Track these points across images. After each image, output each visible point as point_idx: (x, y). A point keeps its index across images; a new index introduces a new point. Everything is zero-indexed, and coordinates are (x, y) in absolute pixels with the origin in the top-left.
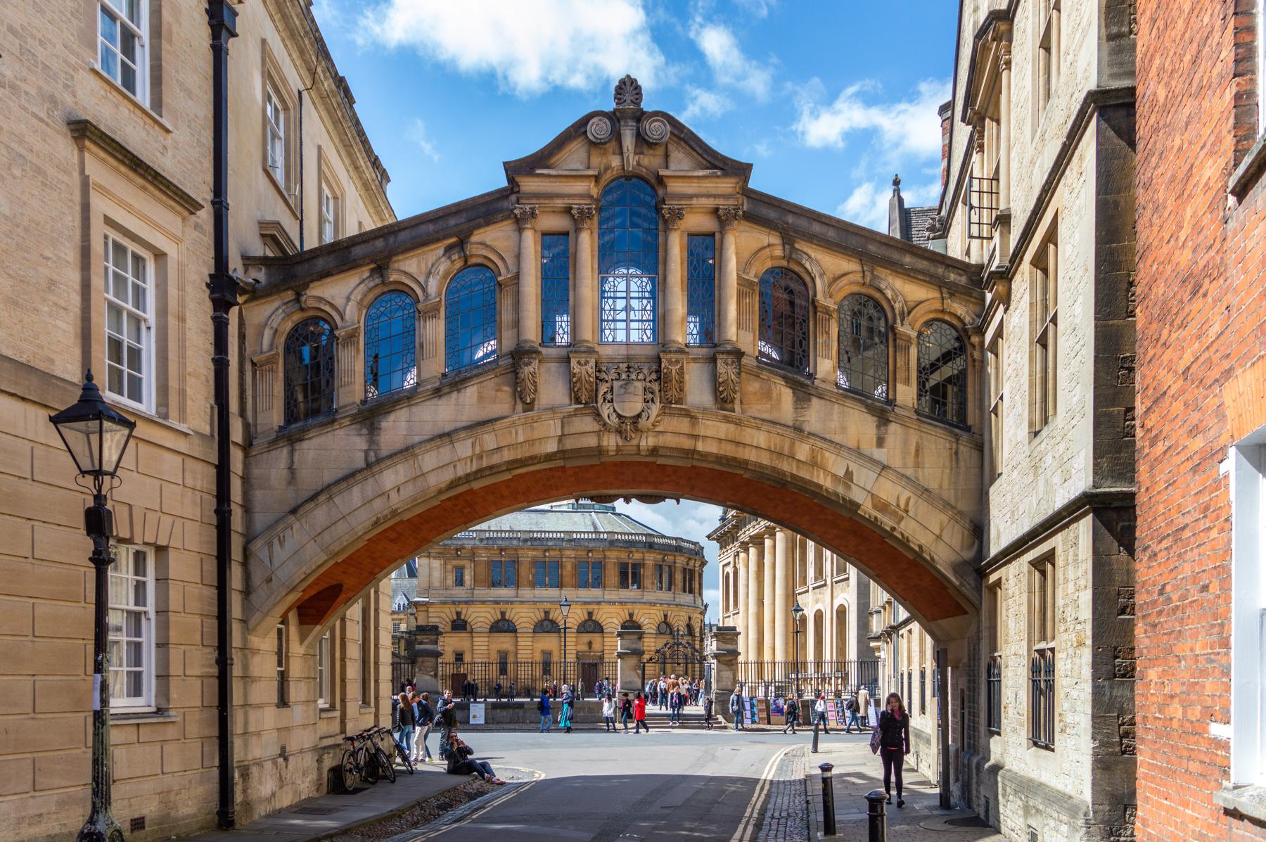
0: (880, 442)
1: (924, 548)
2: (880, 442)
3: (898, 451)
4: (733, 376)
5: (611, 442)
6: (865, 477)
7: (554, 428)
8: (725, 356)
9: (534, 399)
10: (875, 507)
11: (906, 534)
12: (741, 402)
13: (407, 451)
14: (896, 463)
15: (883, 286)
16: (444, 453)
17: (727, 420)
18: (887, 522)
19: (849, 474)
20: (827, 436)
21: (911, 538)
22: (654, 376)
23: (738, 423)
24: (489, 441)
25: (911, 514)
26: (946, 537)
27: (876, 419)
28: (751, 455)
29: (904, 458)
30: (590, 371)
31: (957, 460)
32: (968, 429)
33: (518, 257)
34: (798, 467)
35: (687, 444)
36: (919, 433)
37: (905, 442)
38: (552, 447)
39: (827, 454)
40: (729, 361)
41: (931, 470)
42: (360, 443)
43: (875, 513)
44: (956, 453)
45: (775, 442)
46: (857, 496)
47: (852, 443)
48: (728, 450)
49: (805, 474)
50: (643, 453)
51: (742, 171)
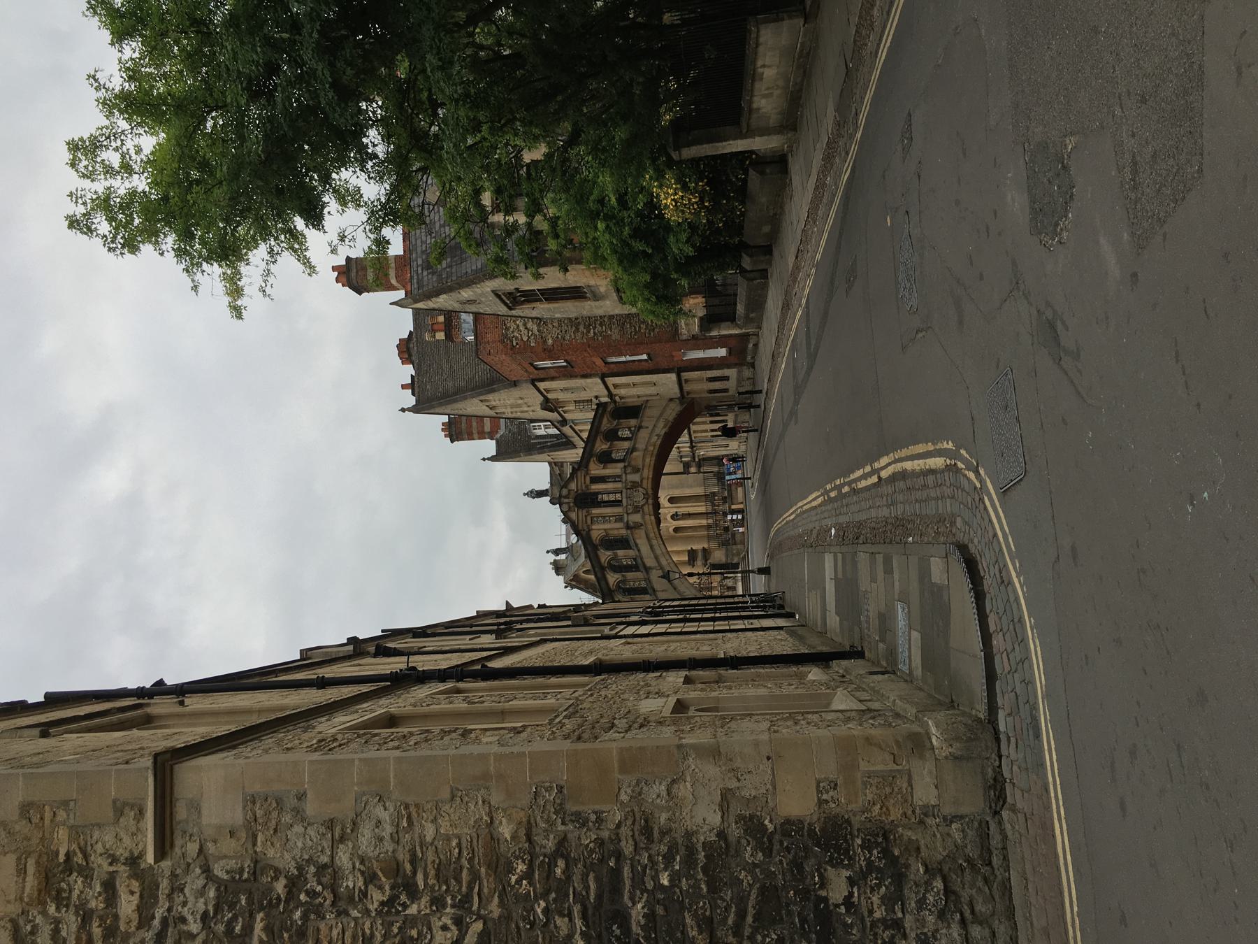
0: (647, 427)
2: (647, 427)
5: (650, 501)
6: (657, 431)
7: (647, 517)
13: (657, 558)
14: (653, 423)
16: (656, 547)
18: (670, 424)
23: (643, 466)
24: (652, 535)
28: (653, 463)
33: (599, 530)
35: (650, 480)
38: (653, 518)
42: (654, 571)
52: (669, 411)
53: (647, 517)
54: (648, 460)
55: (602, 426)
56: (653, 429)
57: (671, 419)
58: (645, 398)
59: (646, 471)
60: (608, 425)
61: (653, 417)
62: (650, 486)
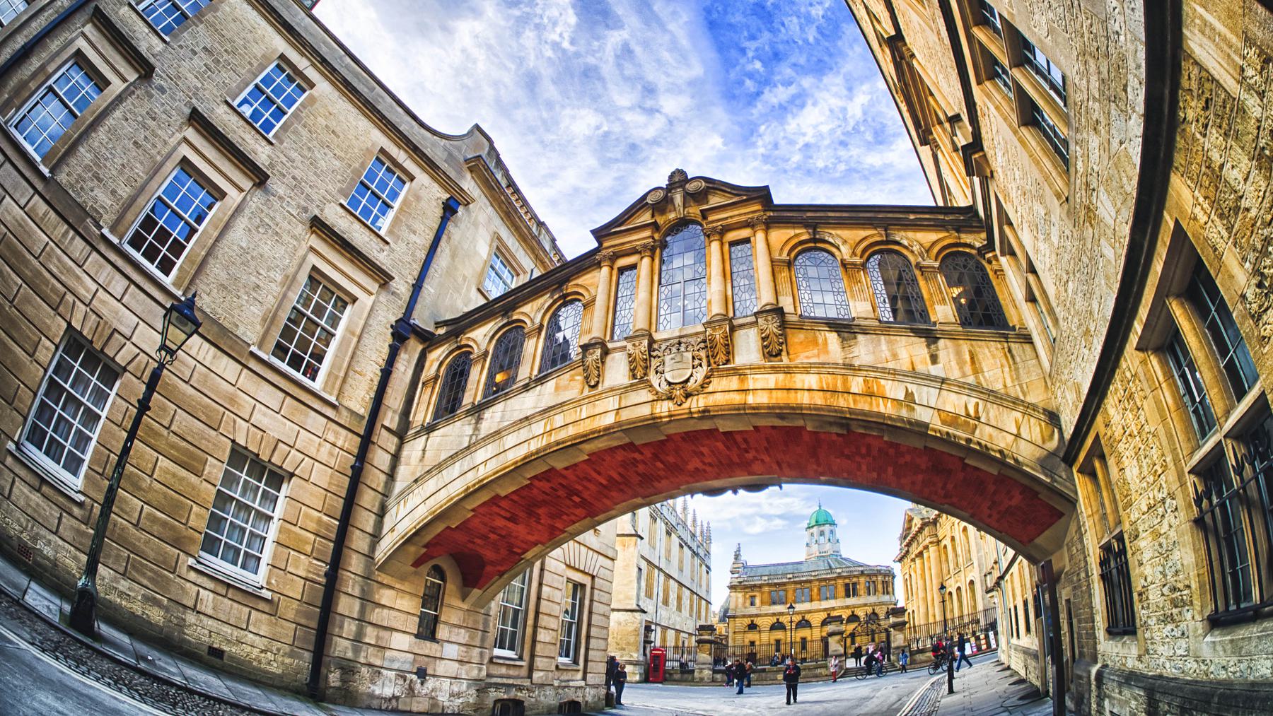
0: (934, 359)
1: (1006, 452)
2: (934, 359)
3: (953, 363)
4: (775, 330)
5: (664, 408)
6: (926, 394)
8: (765, 315)
9: (598, 382)
10: (944, 422)
11: (983, 443)
12: (788, 353)
14: (955, 374)
15: (898, 239)
17: (775, 370)
18: (962, 434)
19: (909, 395)
20: (879, 365)
21: (989, 445)
22: (702, 345)
25: (983, 420)
26: (1024, 435)
27: (923, 339)
28: (804, 399)
29: (961, 368)
30: (643, 349)
31: (1013, 357)
32: (1014, 328)
34: (855, 401)
35: (737, 399)
36: (969, 342)
37: (958, 353)
39: (883, 382)
40: (770, 318)
41: (991, 373)
43: (945, 429)
44: (1010, 351)
45: (827, 381)
46: (923, 415)
47: (906, 366)
48: (780, 398)
49: (863, 405)
50: (696, 415)
51: (762, 195)
52: (1010, 419)
53: (612, 403)
54: (812, 380)
55: (910, 234)
56: (930, 378)
57: (984, 435)
58: (1032, 324)
59: (771, 380)
60: (916, 248)
61: (977, 371)
62: (719, 399)
